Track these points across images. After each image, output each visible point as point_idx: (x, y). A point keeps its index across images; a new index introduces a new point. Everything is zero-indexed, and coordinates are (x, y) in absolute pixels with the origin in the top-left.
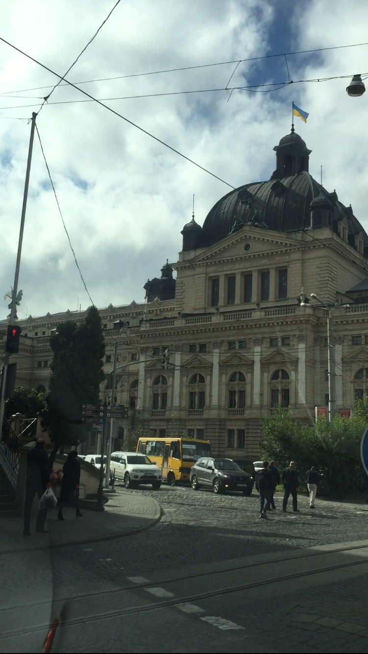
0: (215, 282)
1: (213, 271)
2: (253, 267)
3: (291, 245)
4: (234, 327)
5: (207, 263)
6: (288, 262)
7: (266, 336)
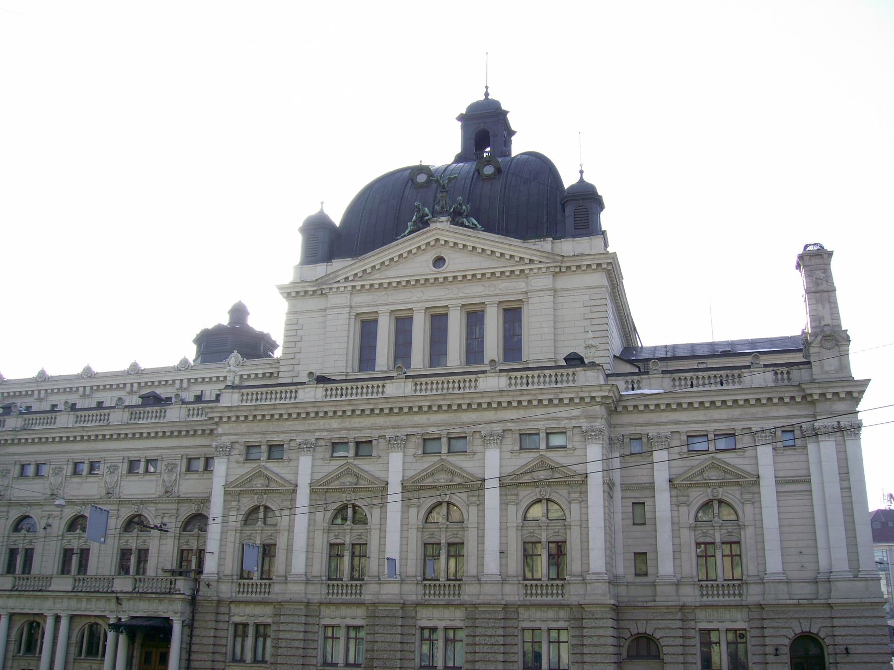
1: (364, 302)
2: (453, 300)
3: (531, 261)
4: (440, 406)
5: (354, 287)
6: (526, 293)
7: (510, 426)
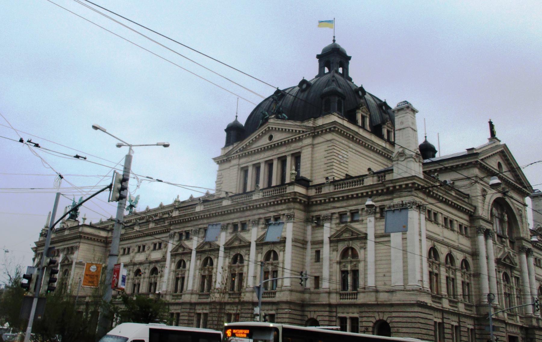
0: (245, 170)
3: (303, 132)
5: (239, 155)
6: (301, 148)
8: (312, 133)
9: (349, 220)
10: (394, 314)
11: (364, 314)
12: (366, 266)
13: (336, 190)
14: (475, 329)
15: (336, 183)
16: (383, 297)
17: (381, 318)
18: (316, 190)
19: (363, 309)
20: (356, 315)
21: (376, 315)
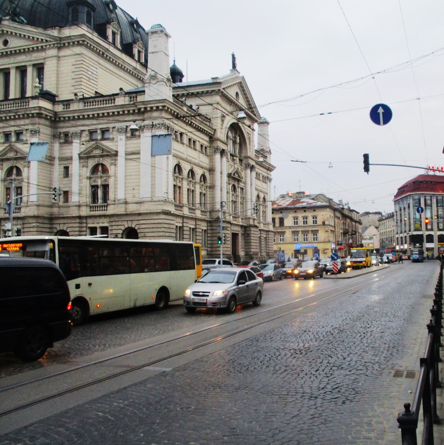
3: (47, 41)
6: (44, 59)
8: (58, 44)
9: (99, 137)
10: (142, 222)
11: (113, 224)
12: (116, 181)
13: (86, 108)
14: (207, 230)
15: (86, 101)
16: (132, 208)
17: (130, 226)
18: (64, 105)
19: (112, 219)
20: (106, 225)
21: (125, 223)
